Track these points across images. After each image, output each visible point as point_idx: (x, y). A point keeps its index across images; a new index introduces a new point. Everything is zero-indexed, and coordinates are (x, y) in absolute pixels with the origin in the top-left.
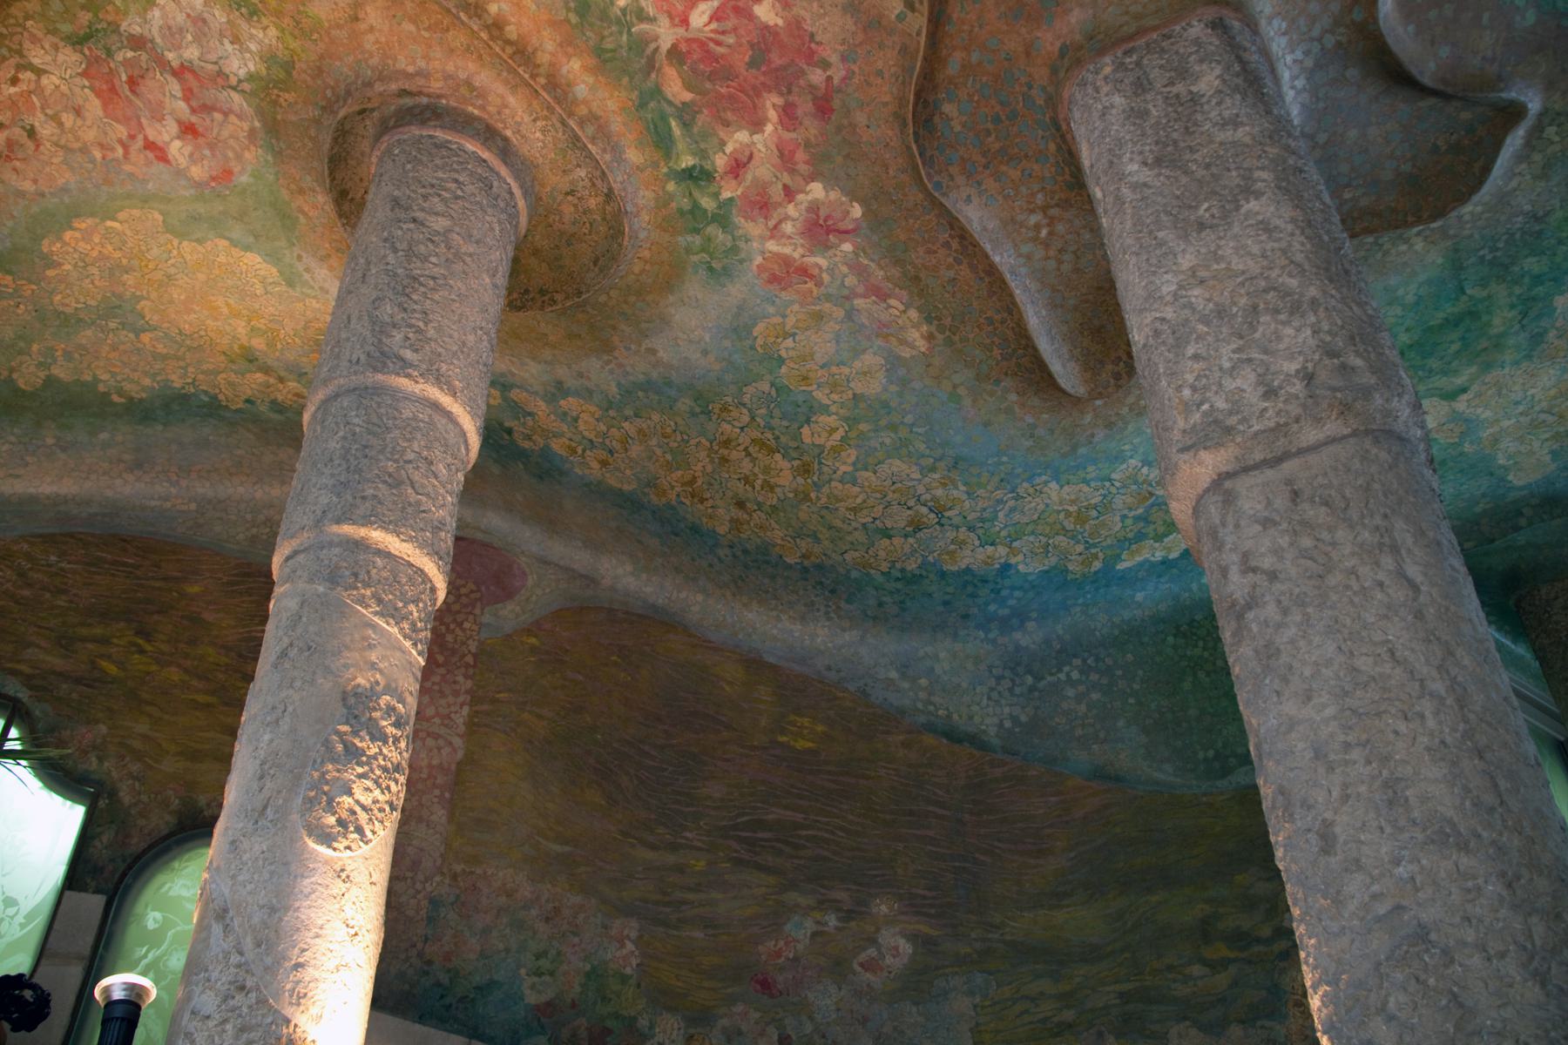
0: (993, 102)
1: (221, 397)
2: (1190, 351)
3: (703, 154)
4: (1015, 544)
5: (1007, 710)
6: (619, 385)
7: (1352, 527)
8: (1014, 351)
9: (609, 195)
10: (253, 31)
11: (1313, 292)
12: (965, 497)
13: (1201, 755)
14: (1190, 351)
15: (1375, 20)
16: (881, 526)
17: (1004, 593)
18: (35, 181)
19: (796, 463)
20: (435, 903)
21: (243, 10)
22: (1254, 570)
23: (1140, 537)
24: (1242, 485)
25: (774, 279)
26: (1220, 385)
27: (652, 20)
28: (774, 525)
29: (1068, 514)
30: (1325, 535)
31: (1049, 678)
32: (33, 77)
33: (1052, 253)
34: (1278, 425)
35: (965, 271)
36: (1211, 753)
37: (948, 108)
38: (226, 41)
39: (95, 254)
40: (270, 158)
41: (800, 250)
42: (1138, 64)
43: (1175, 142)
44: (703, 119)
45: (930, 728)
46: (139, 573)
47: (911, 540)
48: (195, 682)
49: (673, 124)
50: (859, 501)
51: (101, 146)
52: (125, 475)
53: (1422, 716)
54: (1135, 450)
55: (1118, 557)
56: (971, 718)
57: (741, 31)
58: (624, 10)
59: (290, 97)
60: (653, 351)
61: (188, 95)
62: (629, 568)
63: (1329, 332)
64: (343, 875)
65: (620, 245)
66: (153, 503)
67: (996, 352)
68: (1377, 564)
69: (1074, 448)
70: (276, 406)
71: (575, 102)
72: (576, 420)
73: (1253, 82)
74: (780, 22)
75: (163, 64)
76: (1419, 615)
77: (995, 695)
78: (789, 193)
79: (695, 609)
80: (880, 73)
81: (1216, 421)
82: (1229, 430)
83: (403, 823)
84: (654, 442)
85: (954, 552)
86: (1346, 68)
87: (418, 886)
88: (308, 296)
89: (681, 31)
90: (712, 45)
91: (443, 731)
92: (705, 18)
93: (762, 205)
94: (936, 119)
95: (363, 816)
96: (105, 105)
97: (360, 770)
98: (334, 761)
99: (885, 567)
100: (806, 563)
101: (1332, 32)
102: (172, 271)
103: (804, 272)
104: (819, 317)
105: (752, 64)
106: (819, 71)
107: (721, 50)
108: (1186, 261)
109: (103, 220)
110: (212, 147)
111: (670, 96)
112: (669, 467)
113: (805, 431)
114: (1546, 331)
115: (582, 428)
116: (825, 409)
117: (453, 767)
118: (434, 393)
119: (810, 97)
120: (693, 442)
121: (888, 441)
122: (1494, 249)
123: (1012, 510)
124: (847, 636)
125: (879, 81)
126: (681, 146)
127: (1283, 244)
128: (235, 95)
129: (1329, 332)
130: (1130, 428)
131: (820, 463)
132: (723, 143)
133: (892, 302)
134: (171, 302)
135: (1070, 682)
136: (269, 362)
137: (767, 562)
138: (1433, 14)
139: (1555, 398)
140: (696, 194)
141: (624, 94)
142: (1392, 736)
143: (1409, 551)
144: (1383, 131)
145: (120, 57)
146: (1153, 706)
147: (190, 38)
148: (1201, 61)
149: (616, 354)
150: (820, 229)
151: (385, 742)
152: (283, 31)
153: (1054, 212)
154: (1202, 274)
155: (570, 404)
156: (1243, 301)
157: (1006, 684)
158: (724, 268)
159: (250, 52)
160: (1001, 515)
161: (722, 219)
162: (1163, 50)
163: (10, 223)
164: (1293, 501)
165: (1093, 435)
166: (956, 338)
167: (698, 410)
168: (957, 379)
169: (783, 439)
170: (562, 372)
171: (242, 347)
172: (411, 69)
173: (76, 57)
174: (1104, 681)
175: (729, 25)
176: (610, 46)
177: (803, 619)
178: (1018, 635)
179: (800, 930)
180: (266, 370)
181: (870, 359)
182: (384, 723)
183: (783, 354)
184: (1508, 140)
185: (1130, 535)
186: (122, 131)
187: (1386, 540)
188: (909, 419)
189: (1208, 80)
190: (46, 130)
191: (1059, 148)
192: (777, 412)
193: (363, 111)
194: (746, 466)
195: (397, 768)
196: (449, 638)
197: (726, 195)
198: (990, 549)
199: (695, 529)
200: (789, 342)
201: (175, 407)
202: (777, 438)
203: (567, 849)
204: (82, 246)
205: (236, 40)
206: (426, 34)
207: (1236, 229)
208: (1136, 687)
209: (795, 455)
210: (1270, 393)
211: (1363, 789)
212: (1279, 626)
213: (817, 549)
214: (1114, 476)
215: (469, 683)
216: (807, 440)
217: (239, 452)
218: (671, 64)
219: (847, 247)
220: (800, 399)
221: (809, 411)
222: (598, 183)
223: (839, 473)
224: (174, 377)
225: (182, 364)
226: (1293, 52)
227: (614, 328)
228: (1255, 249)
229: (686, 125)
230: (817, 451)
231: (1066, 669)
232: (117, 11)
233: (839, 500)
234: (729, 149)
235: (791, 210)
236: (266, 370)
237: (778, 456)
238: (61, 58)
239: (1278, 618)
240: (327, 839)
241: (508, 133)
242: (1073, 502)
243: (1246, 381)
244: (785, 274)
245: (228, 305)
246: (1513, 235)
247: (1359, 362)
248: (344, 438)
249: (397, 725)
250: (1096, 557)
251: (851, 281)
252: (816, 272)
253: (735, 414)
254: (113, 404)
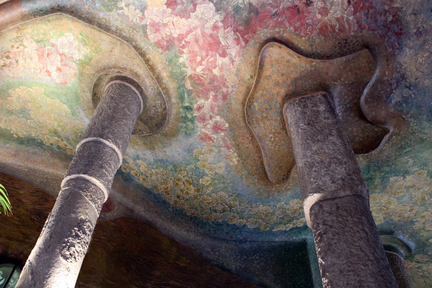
0: (267, 105)
1: (44, 142)
2: (314, 169)
3: (191, 103)
4: (248, 220)
5: (238, 264)
6: (154, 159)
7: (352, 217)
8: (259, 168)
9: (165, 109)
10: (84, 49)
11: (345, 160)
12: (238, 205)
13: (288, 284)
14: (314, 169)
15: (359, 103)
16: (214, 209)
17: (243, 232)
18: (13, 74)
19: (196, 188)
21: (83, 43)
22: (326, 225)
23: (280, 223)
24: (324, 204)
25: (202, 139)
26: (321, 179)
27: (187, 68)
28: (186, 204)
29: (264, 214)
30: (345, 218)
31: (251, 257)
32: (23, 48)
33: (273, 145)
34: (335, 190)
35: (251, 146)
36: (291, 283)
37: (255, 104)
38: (76, 50)
39: (23, 96)
40: (78, 81)
41: (210, 133)
42: (305, 101)
43: (313, 121)
44: (194, 94)
45: (217, 266)
46: (7, 184)
47: (222, 214)
48: (16, 218)
49: (186, 94)
50: (210, 201)
51: (34, 69)
52: (10, 157)
53: (368, 265)
54: (284, 200)
55: (273, 228)
56: (229, 265)
57: (209, 75)
58: (180, 64)
59: (88, 67)
60: (165, 152)
61: (62, 61)
62: (143, 209)
63: (349, 170)
64: (68, 269)
65: (164, 122)
66: (16, 167)
67: (254, 168)
68: (358, 227)
69: (269, 196)
70: (59, 147)
71: (162, 84)
72: (140, 166)
73: (332, 110)
74: (219, 75)
75: (57, 51)
76: (368, 240)
77: (236, 260)
78: (211, 117)
79: (159, 223)
80: (240, 92)
81: (319, 187)
82: (322, 190)
83: (85, 259)
84: (159, 176)
85: (232, 219)
86: (351, 113)
88: (77, 119)
89: (193, 72)
90: (200, 77)
92: (200, 70)
93: (203, 119)
94: (252, 106)
95: (76, 254)
96: (39, 59)
97: (78, 241)
98: (73, 237)
99: (213, 220)
100: (192, 216)
101: (349, 104)
102: (42, 105)
103: (210, 138)
104: (211, 151)
105: (209, 83)
106: (225, 89)
107: (202, 78)
108: (314, 148)
109: (28, 88)
110: (64, 75)
111: (186, 87)
112: (162, 183)
113: (201, 180)
114: (387, 186)
115: (141, 169)
116: (207, 175)
118: (114, 147)
119: (222, 94)
120: (170, 178)
121: (222, 186)
122: (378, 163)
123: (250, 210)
124: (199, 238)
125: (240, 94)
127: (339, 148)
128: (74, 63)
129: (349, 170)
130: (284, 194)
131: (202, 189)
132: (197, 101)
133: (231, 150)
134: (39, 113)
135: (256, 259)
136: (61, 135)
137: (182, 214)
138: (372, 104)
139: (387, 203)
140: (187, 113)
141: (175, 84)
142: (360, 270)
143: (366, 225)
144: (357, 130)
145: (47, 48)
146: (277, 269)
147: (67, 47)
148: (321, 103)
149: (155, 151)
150: (217, 128)
151: (86, 235)
152: (92, 50)
153: (276, 134)
154: (318, 152)
155: (139, 162)
156: (328, 160)
157: (239, 257)
158: (190, 134)
159: (82, 54)
160: (246, 211)
161: (192, 121)
162: (311, 99)
163: (2, 83)
164: (337, 209)
165: (274, 194)
166: (245, 162)
167: (173, 169)
168: (243, 173)
169: (194, 181)
170: (139, 153)
171: (54, 129)
172: (122, 67)
173: (36, 45)
174: (265, 260)
175: (206, 73)
176: (175, 72)
177: (188, 231)
178: (244, 245)
180: (59, 137)
181: (222, 164)
182: (86, 230)
183: (200, 159)
184: (385, 137)
185: (278, 222)
186: (41, 66)
187: (360, 221)
188: (228, 181)
189: (322, 108)
190: (21, 61)
191: (281, 119)
192: (194, 174)
193: (107, 74)
194: (183, 187)
195: (87, 243)
197: (195, 115)
198: (242, 220)
199: (164, 202)
200: (202, 156)
201: (31, 142)
202: (193, 181)
203: (113, 283)
204: (20, 93)
205: (79, 50)
206: (128, 59)
207: (327, 143)
208: (273, 263)
209: (196, 186)
210: (333, 182)
211: (353, 282)
212: (332, 239)
213: (196, 213)
214: (277, 206)
216: (200, 182)
217: (44, 158)
218: (189, 79)
219: (223, 134)
220: (201, 171)
221: (203, 175)
222: (163, 105)
223: (207, 193)
224: (33, 133)
225: (36, 130)
226: (339, 106)
227: (157, 144)
228: (332, 148)
229: (189, 95)
230: (202, 186)
231: (255, 256)
232: (50, 37)
233: (205, 200)
234: (198, 103)
235: (210, 122)
236: (59, 137)
237: (192, 186)
238: (32, 45)
239: (332, 237)
240: (66, 258)
241: (143, 88)
242: (265, 211)
243: (327, 179)
244: (205, 138)
245: (54, 117)
246: (383, 160)
247: (355, 178)
248: (89, 153)
249: (90, 231)
250: (268, 227)
251: (221, 143)
252: (213, 139)
253: (183, 172)
254: (13, 137)
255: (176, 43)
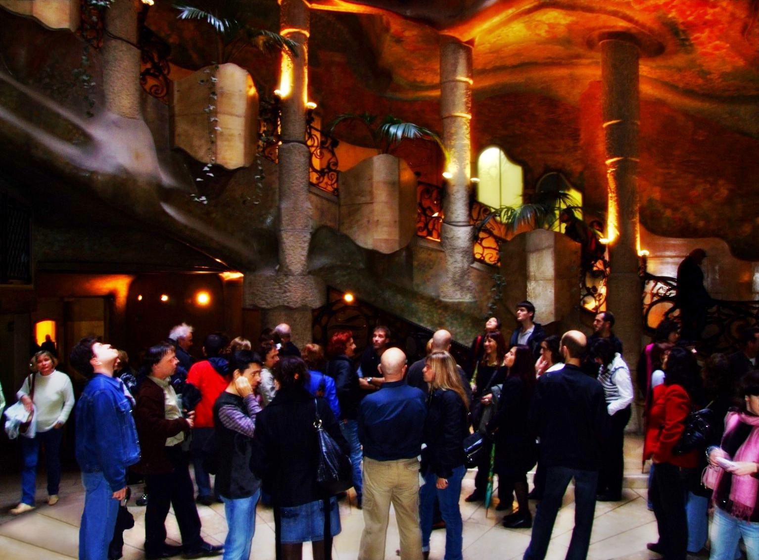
179: (699, 189)
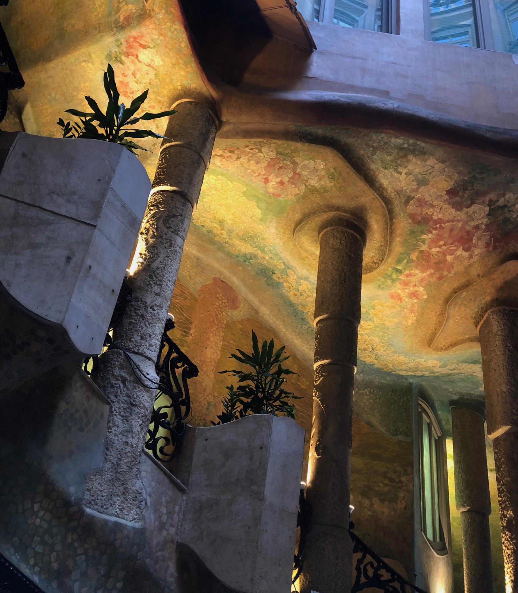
20: (209, 403)
37: (464, 293)
49: (405, 260)
58: (421, 239)
78: (415, 286)
87: (205, 397)
89: (428, 249)
91: (215, 348)
103: (400, 299)
116: (373, 322)
117: (217, 361)
126: (402, 265)
132: (412, 270)
159: (320, 183)
196: (219, 316)
215: (223, 334)
219: (415, 301)
229: (408, 262)
255: (431, 223)
